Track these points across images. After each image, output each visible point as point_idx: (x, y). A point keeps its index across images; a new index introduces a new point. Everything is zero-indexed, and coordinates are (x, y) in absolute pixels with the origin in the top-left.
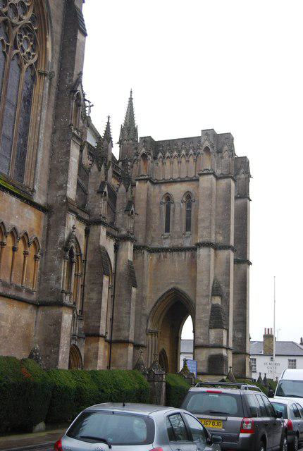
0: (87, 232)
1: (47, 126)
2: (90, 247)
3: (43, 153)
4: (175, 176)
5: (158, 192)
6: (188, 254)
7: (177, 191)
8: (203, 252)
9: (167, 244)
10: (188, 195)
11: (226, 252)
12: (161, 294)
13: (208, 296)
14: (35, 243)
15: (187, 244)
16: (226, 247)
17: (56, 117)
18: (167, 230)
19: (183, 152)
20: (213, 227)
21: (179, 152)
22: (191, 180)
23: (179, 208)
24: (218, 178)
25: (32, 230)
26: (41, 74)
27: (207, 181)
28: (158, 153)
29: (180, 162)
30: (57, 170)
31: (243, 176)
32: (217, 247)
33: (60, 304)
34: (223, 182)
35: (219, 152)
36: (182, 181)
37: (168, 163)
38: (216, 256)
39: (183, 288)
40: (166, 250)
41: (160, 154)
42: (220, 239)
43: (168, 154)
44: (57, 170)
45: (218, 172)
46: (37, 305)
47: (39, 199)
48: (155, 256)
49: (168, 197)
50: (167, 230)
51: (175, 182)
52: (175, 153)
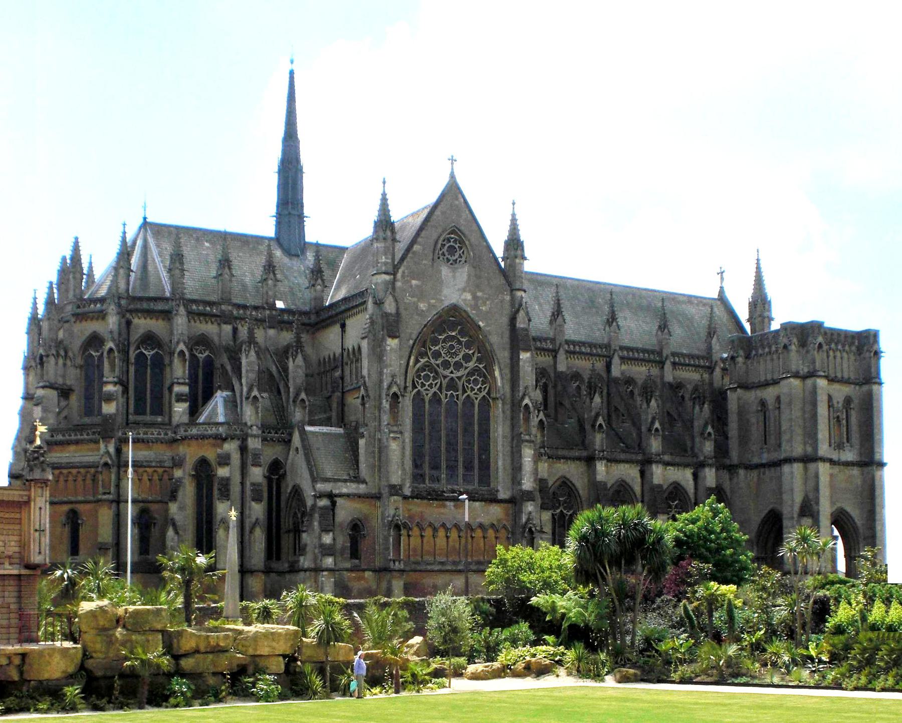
0: (642, 473)
1: (496, 442)
2: (647, 487)
3: (504, 460)
5: (752, 396)
12: (763, 515)
13: (792, 518)
14: (504, 527)
21: (770, 347)
25: (499, 521)
26: (494, 399)
28: (751, 351)
29: (772, 360)
34: (809, 382)
37: (762, 362)
41: (754, 352)
42: (809, 449)
43: (760, 351)
47: (503, 495)
48: (754, 474)
49: (763, 403)
52: (767, 350)
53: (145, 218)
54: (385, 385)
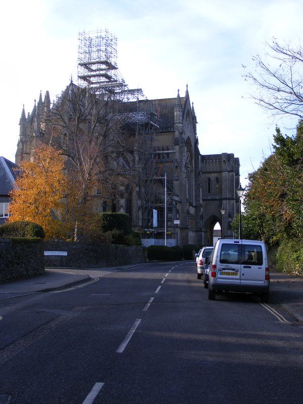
4: (211, 170)
6: (218, 202)
7: (213, 176)
8: (224, 202)
9: (209, 198)
10: (217, 179)
11: (232, 201)
15: (217, 198)
16: (233, 199)
17: (195, 181)
18: (209, 192)
19: (214, 161)
20: (228, 192)
21: (212, 160)
22: (218, 172)
23: (213, 182)
24: (229, 172)
27: (225, 174)
30: (197, 196)
31: (237, 166)
32: (229, 199)
33: (202, 231)
34: (231, 173)
35: (229, 161)
36: (214, 172)
38: (229, 203)
39: (216, 214)
40: (209, 200)
42: (230, 196)
44: (197, 196)
45: (229, 169)
46: (196, 231)
49: (209, 179)
50: (209, 192)
51: (211, 172)
53: (72, 81)
54: (184, 163)
